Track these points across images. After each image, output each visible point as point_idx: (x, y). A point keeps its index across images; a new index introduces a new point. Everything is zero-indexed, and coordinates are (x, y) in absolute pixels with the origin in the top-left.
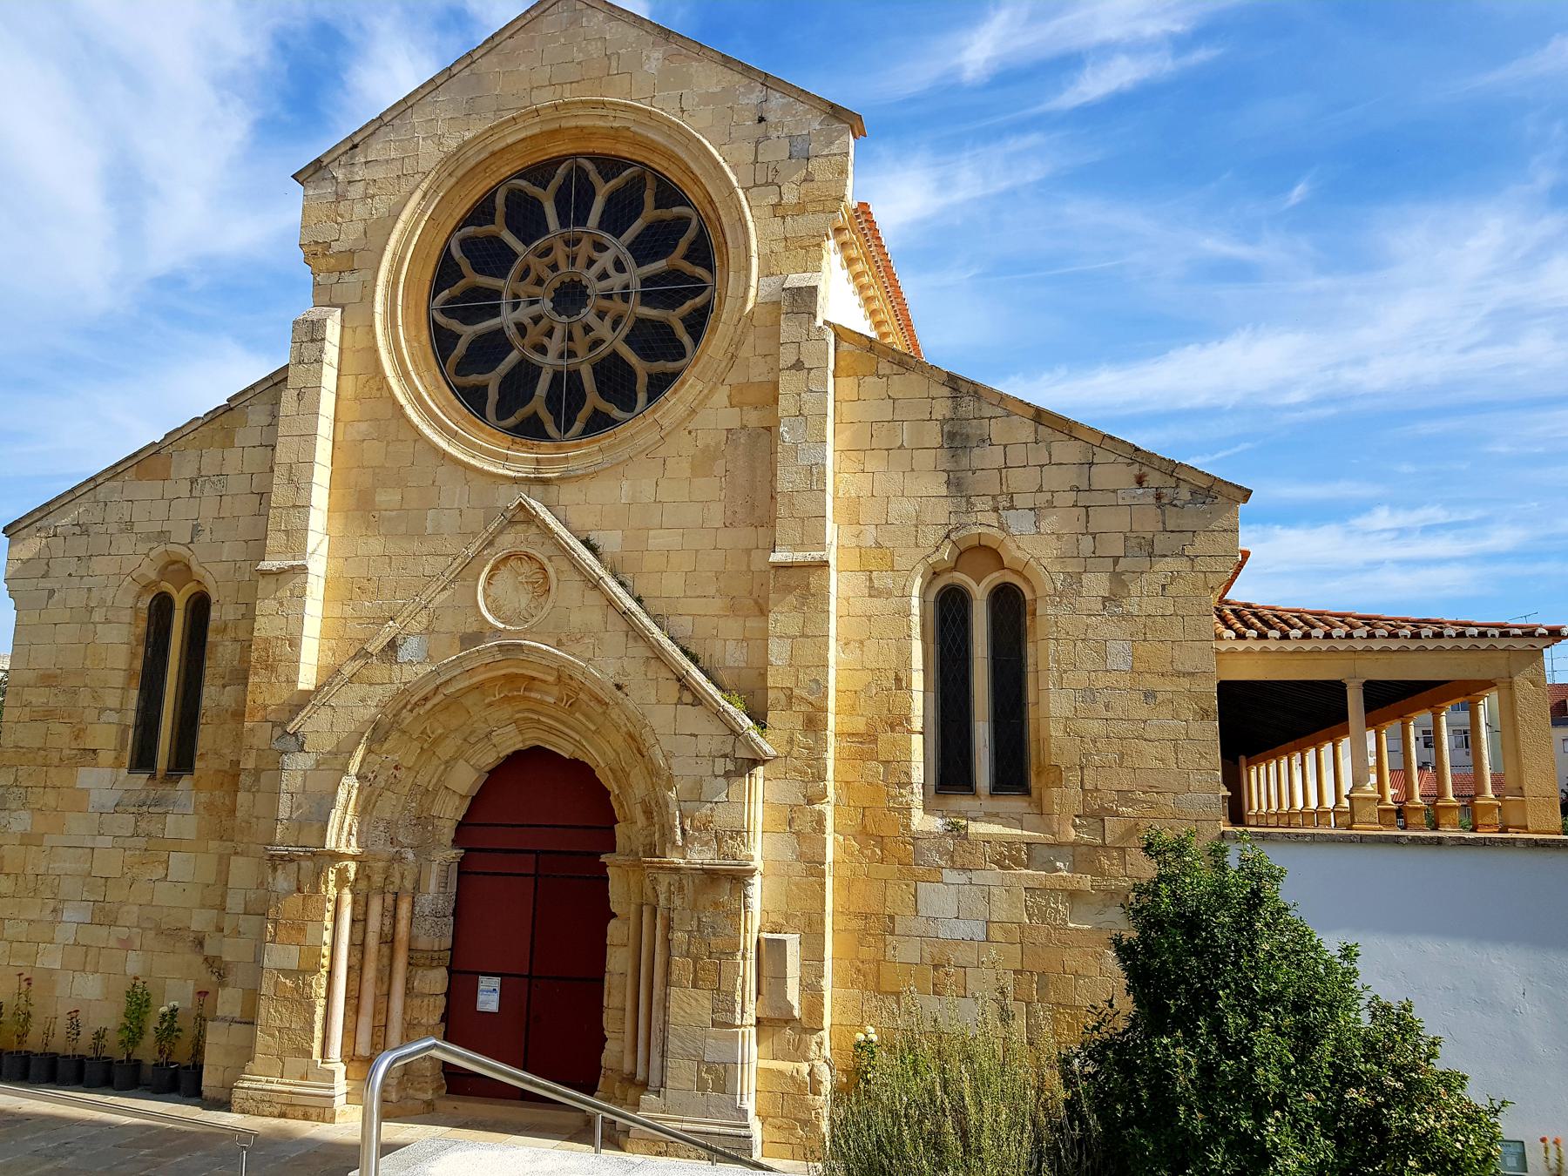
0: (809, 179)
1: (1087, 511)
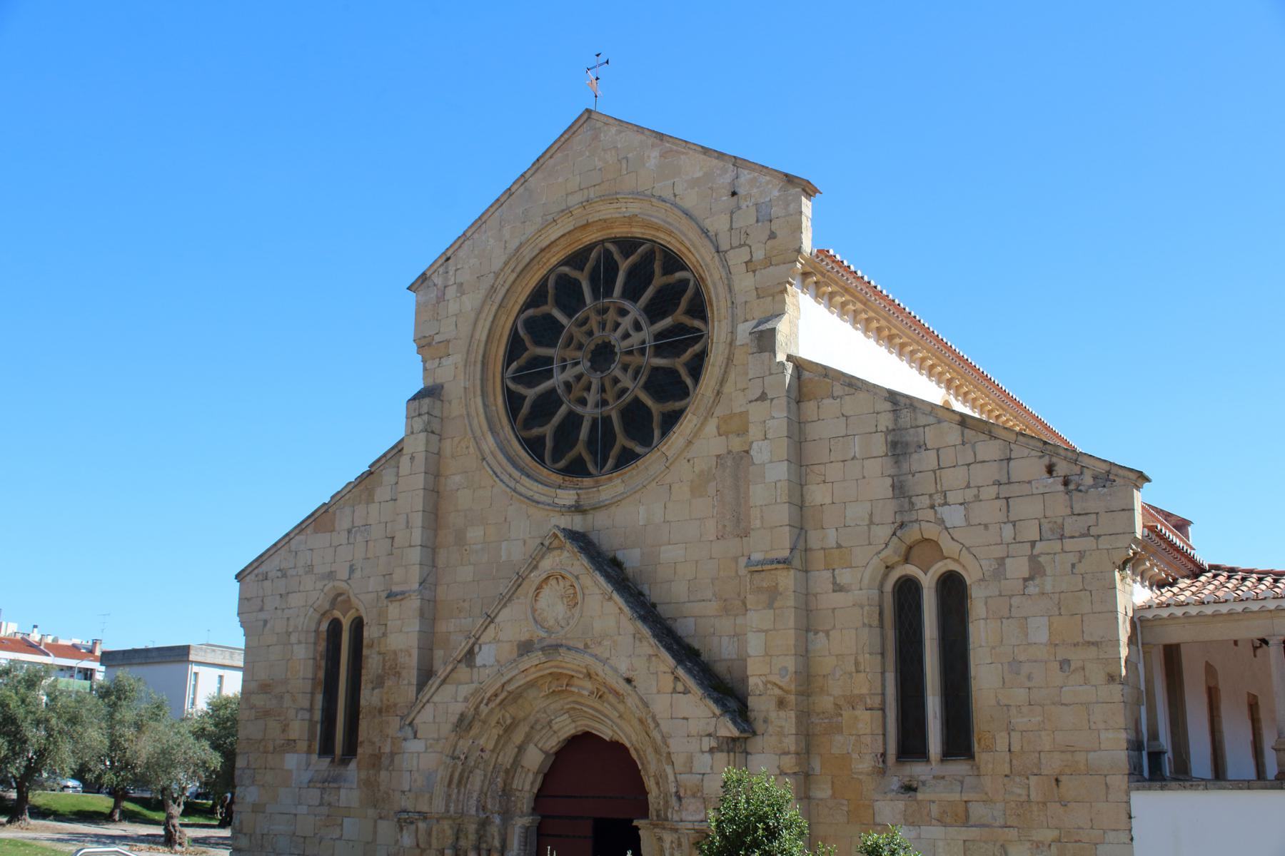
0: (772, 236)
1: (1008, 502)
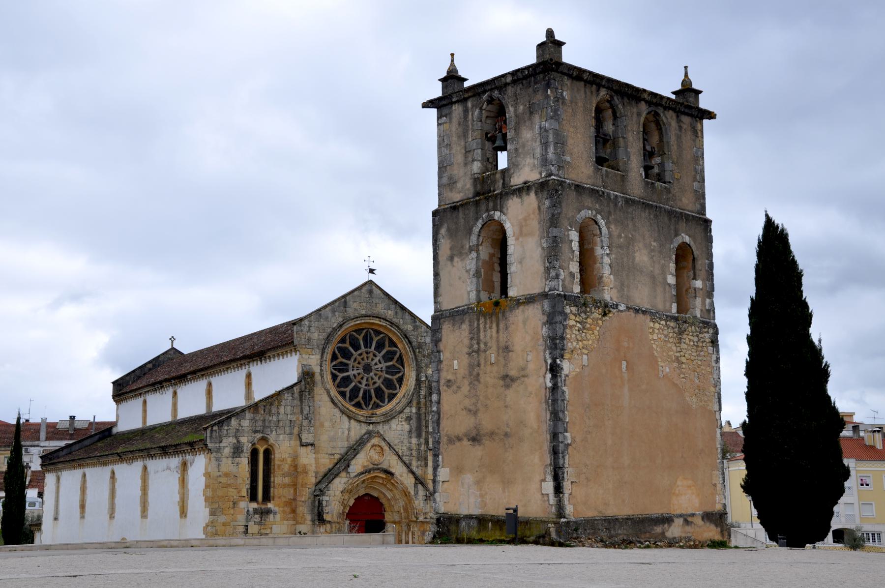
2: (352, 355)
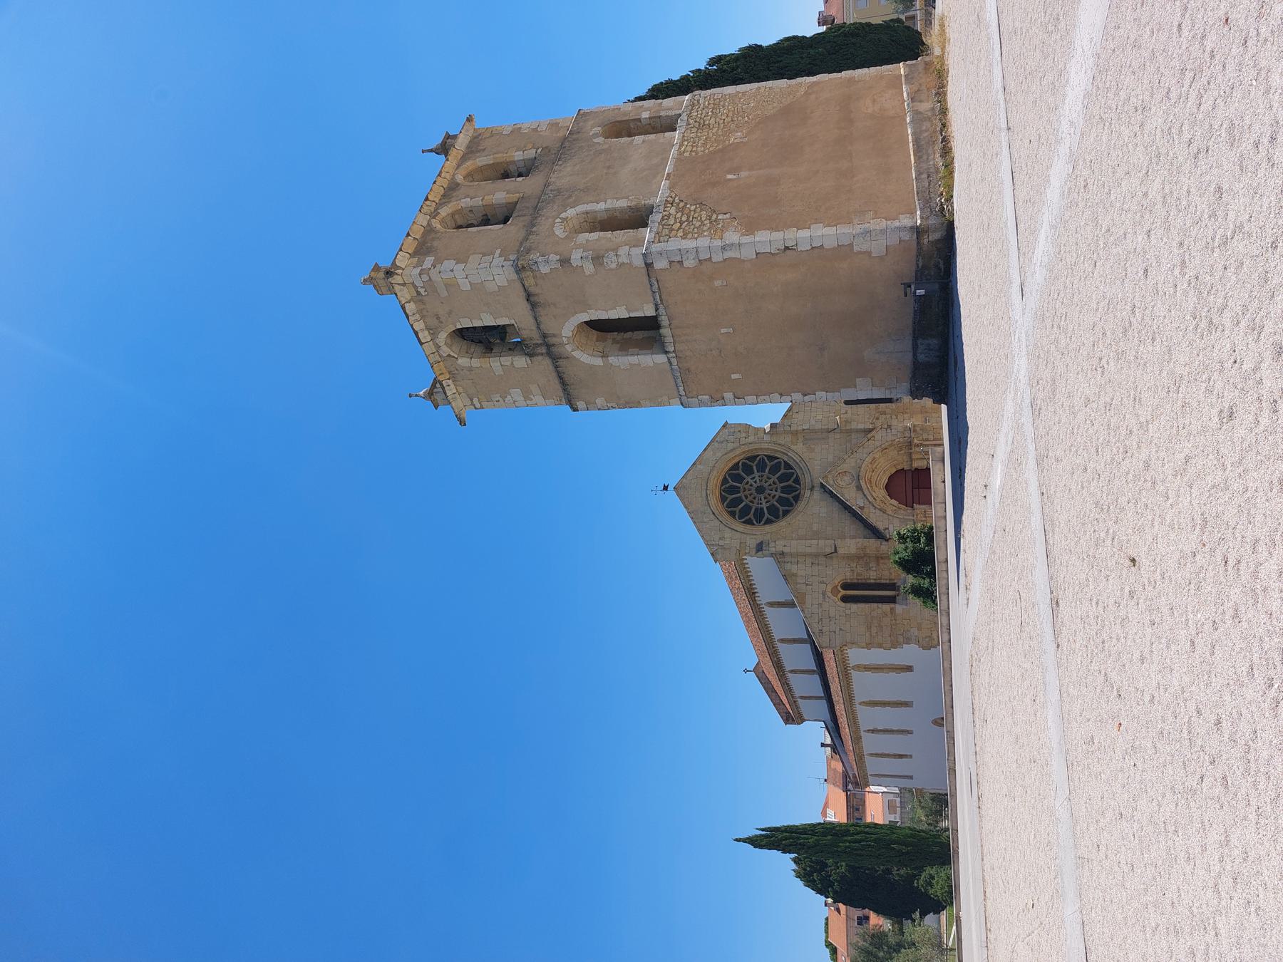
0: (740, 431)
2: (746, 505)
